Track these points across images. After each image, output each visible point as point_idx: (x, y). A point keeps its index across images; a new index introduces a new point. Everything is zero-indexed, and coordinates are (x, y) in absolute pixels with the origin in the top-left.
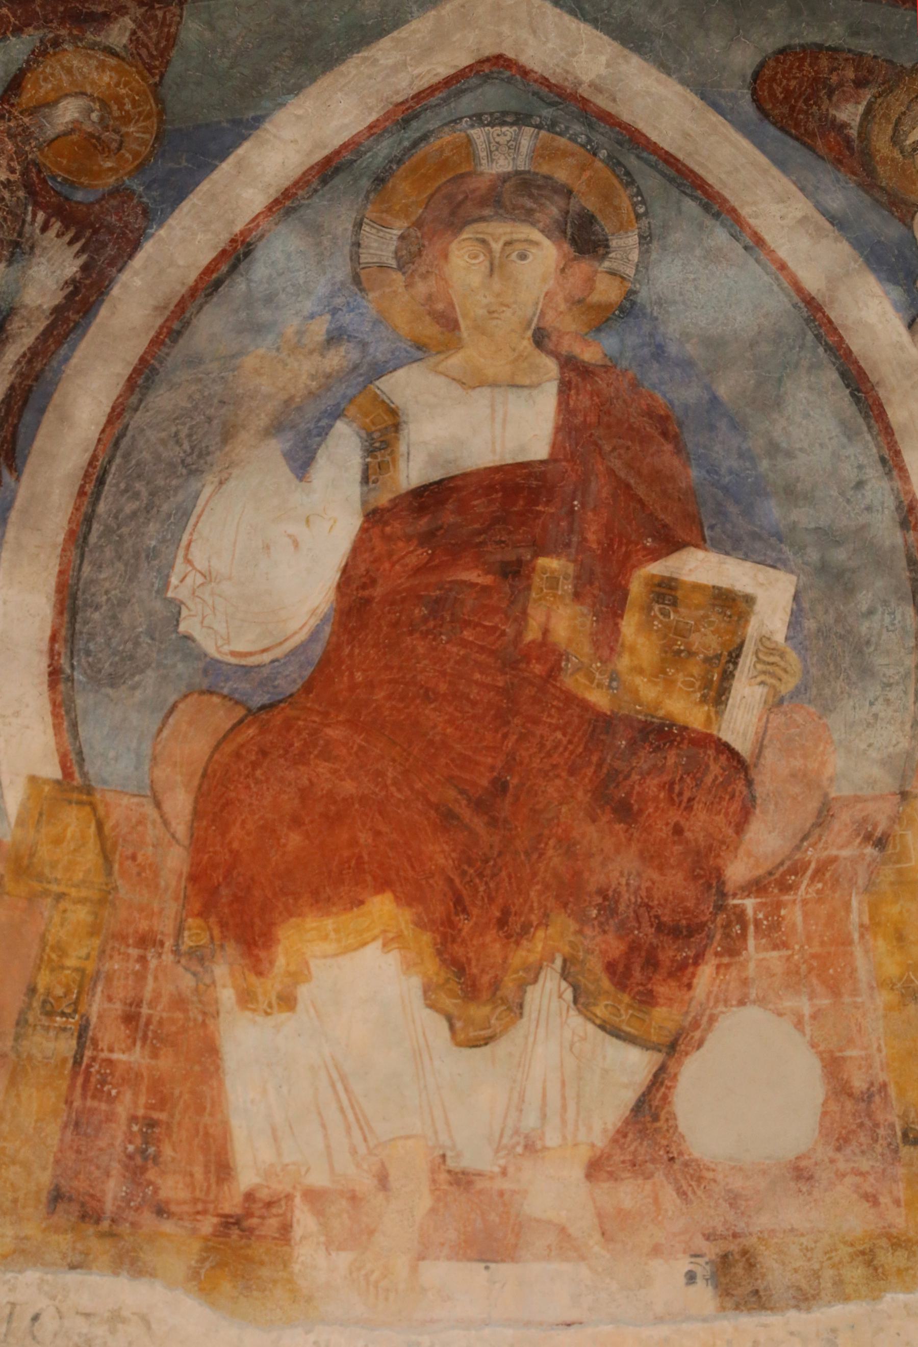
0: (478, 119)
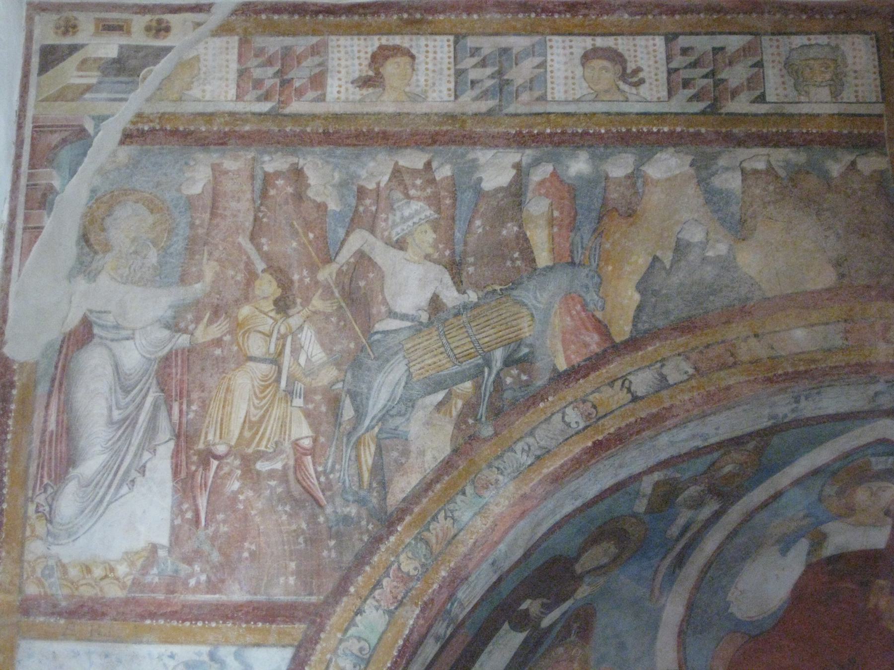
0: (874, 455)
